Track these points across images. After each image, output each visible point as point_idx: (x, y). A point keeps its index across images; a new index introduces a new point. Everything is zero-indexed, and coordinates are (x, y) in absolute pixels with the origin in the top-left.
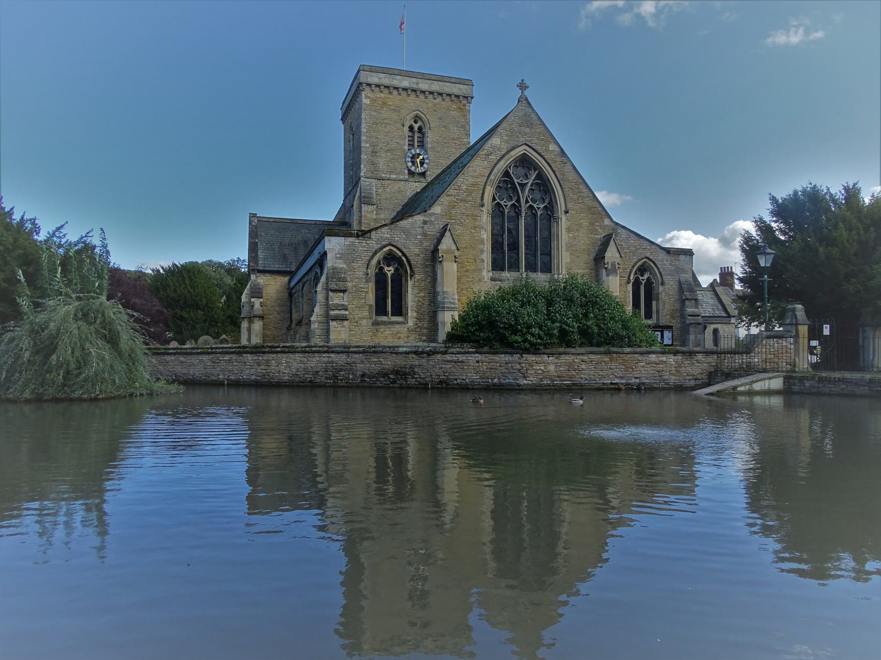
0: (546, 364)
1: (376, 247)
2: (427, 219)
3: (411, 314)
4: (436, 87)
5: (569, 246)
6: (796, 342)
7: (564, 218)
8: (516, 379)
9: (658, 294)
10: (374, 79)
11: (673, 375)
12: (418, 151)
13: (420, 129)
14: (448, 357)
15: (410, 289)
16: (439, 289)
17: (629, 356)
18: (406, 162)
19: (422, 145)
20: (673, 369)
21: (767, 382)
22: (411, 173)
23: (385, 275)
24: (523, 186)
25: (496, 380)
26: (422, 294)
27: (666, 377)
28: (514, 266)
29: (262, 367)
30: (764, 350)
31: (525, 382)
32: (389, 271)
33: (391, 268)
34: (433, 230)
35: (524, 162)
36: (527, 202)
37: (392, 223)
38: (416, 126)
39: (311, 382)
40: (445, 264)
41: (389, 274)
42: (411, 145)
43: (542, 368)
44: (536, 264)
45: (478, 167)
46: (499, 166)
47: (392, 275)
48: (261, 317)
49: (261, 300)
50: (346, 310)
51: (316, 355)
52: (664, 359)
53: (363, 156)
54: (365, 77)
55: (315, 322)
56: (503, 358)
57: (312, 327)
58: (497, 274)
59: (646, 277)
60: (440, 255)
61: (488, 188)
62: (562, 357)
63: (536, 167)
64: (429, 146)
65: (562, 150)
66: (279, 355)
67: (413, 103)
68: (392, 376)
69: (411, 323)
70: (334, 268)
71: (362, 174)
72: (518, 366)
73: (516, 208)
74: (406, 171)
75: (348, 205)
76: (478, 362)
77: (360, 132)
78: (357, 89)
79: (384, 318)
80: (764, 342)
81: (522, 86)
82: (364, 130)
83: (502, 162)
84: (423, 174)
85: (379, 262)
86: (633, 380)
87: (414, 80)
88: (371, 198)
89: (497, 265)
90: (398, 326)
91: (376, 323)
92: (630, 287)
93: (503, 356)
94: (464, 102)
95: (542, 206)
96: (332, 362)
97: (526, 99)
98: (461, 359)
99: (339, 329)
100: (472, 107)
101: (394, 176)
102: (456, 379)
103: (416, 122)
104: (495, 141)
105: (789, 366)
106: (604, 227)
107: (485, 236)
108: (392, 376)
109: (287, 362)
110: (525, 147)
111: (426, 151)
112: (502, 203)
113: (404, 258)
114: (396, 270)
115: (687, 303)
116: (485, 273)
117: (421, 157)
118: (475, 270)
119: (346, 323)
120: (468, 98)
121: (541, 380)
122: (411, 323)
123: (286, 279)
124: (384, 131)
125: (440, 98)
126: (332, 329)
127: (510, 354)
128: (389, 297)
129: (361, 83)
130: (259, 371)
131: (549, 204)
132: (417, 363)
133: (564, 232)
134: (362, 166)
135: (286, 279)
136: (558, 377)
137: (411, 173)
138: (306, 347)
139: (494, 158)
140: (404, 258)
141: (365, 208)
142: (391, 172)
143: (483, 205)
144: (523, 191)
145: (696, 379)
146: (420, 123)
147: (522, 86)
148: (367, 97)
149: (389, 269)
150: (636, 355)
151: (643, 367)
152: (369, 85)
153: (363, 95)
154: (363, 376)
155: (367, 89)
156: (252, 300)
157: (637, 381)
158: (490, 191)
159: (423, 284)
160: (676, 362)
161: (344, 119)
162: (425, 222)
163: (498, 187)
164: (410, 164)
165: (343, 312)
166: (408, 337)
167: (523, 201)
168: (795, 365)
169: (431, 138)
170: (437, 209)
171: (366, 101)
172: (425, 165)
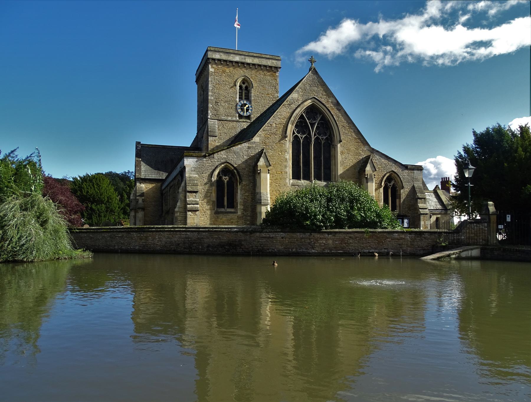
0: (327, 239)
1: (217, 164)
2: (250, 145)
5: (343, 163)
6: (489, 226)
7: (339, 145)
8: (307, 249)
9: (400, 194)
10: (217, 56)
11: (409, 247)
12: (245, 102)
14: (263, 235)
15: (239, 191)
16: (257, 191)
17: (380, 234)
18: (236, 109)
19: (248, 98)
20: (409, 243)
21: (470, 252)
22: (241, 117)
23: (223, 181)
24: (312, 125)
25: (294, 250)
26: (247, 194)
27: (404, 248)
28: (307, 177)
29: (143, 241)
30: (468, 231)
31: (313, 251)
32: (226, 179)
33: (227, 177)
34: (253, 153)
35: (313, 111)
36: (315, 135)
37: (228, 148)
38: (244, 86)
39: (174, 250)
40: (262, 175)
41: (226, 181)
42: (241, 98)
43: (324, 242)
44: (321, 175)
45: (283, 112)
46: (297, 112)
47: (228, 182)
48: (143, 209)
49: (143, 198)
50: (197, 204)
51: (178, 233)
52: (403, 236)
53: (210, 105)
55: (177, 212)
56: (299, 235)
57: (176, 215)
58: (296, 181)
59: (392, 184)
60: (259, 169)
61: (290, 126)
62: (337, 235)
63: (321, 113)
64: (253, 98)
65: (338, 102)
66: (154, 233)
68: (227, 247)
69: (239, 213)
70: (190, 177)
71: (209, 117)
72: (308, 241)
73: (308, 140)
74: (237, 115)
75: (200, 136)
76: (282, 238)
77: (208, 89)
78: (206, 62)
79: (223, 210)
80: (468, 226)
82: (210, 88)
83: (299, 109)
84: (248, 117)
85: (219, 173)
86: (383, 250)
87: (243, 57)
88: (215, 132)
89: (296, 176)
90: (231, 215)
91: (217, 213)
92: (382, 190)
93: (299, 234)
94: (275, 71)
95: (325, 138)
96: (188, 238)
97: (314, 69)
98: (271, 236)
99: (193, 216)
101: (230, 118)
102: (268, 249)
104: (294, 95)
105: (484, 242)
107: (288, 157)
108: (227, 247)
109: (159, 238)
110: (313, 99)
111: (250, 103)
112: (299, 135)
113: (235, 171)
114: (230, 178)
115: (419, 200)
116: (287, 181)
117: (247, 106)
118: (281, 179)
119: (197, 213)
121: (324, 249)
122: (239, 213)
123: (159, 184)
125: (260, 68)
126: (188, 216)
127: (303, 232)
129: (209, 58)
130: (141, 243)
131: (329, 136)
132: (243, 238)
133: (339, 154)
134: (209, 112)
135: (159, 184)
136: (335, 248)
137: (241, 117)
138: (171, 228)
139: (294, 106)
140: (235, 171)
143: (286, 137)
144: (313, 128)
145: (424, 250)
146: (246, 84)
148: (212, 67)
149: (226, 178)
150: (385, 234)
151: (390, 241)
152: (214, 60)
153: (210, 66)
154: (208, 246)
157: (386, 250)
159: (248, 188)
160: (411, 238)
161: (197, 81)
162: (249, 148)
163: (296, 126)
164: (239, 110)
165: (196, 206)
166: (238, 222)
167: (313, 134)
168: (488, 241)
169: (254, 93)
170: (256, 139)
171: (211, 70)
172: (250, 111)
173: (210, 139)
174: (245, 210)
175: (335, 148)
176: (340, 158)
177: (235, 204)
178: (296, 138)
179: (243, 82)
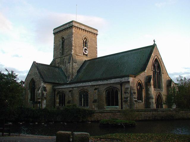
4: (90, 30)
7: (162, 74)
10: (76, 25)
13: (85, 41)
38: (85, 41)
54: (74, 24)
67: (85, 34)
81: (154, 41)
84: (86, 55)
94: (96, 35)
100: (98, 37)
103: (84, 39)
120: (97, 34)
124: (77, 40)
137: (84, 54)
141: (74, 64)
142: (80, 53)
146: (85, 40)
147: (154, 41)
148: (74, 30)
152: (75, 27)
155: (74, 28)
156: (44, 92)
164: (84, 52)
169: (89, 44)
173: (74, 64)
175: (161, 76)
176: (163, 80)
179: (85, 38)
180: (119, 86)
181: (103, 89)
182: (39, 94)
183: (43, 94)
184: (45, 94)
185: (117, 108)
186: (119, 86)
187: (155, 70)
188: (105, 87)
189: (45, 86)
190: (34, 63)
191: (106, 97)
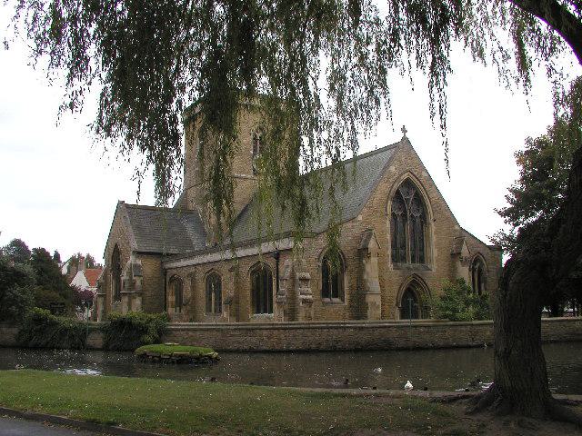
3: (347, 297)
7: (433, 224)
38: (259, 135)
42: (255, 151)
69: (346, 303)
79: (327, 300)
81: (404, 130)
104: (392, 169)
106: (456, 231)
128: (331, 287)
147: (404, 130)
158: (390, 203)
174: (351, 301)
176: (434, 238)
177: (340, 292)
178: (393, 214)
180: (271, 263)
181: (245, 269)
182: (124, 283)
183: (133, 284)
184: (138, 283)
185: (269, 318)
186: (271, 263)
187: (405, 211)
188: (251, 264)
189: (139, 262)
190: (121, 203)
191: (253, 291)
